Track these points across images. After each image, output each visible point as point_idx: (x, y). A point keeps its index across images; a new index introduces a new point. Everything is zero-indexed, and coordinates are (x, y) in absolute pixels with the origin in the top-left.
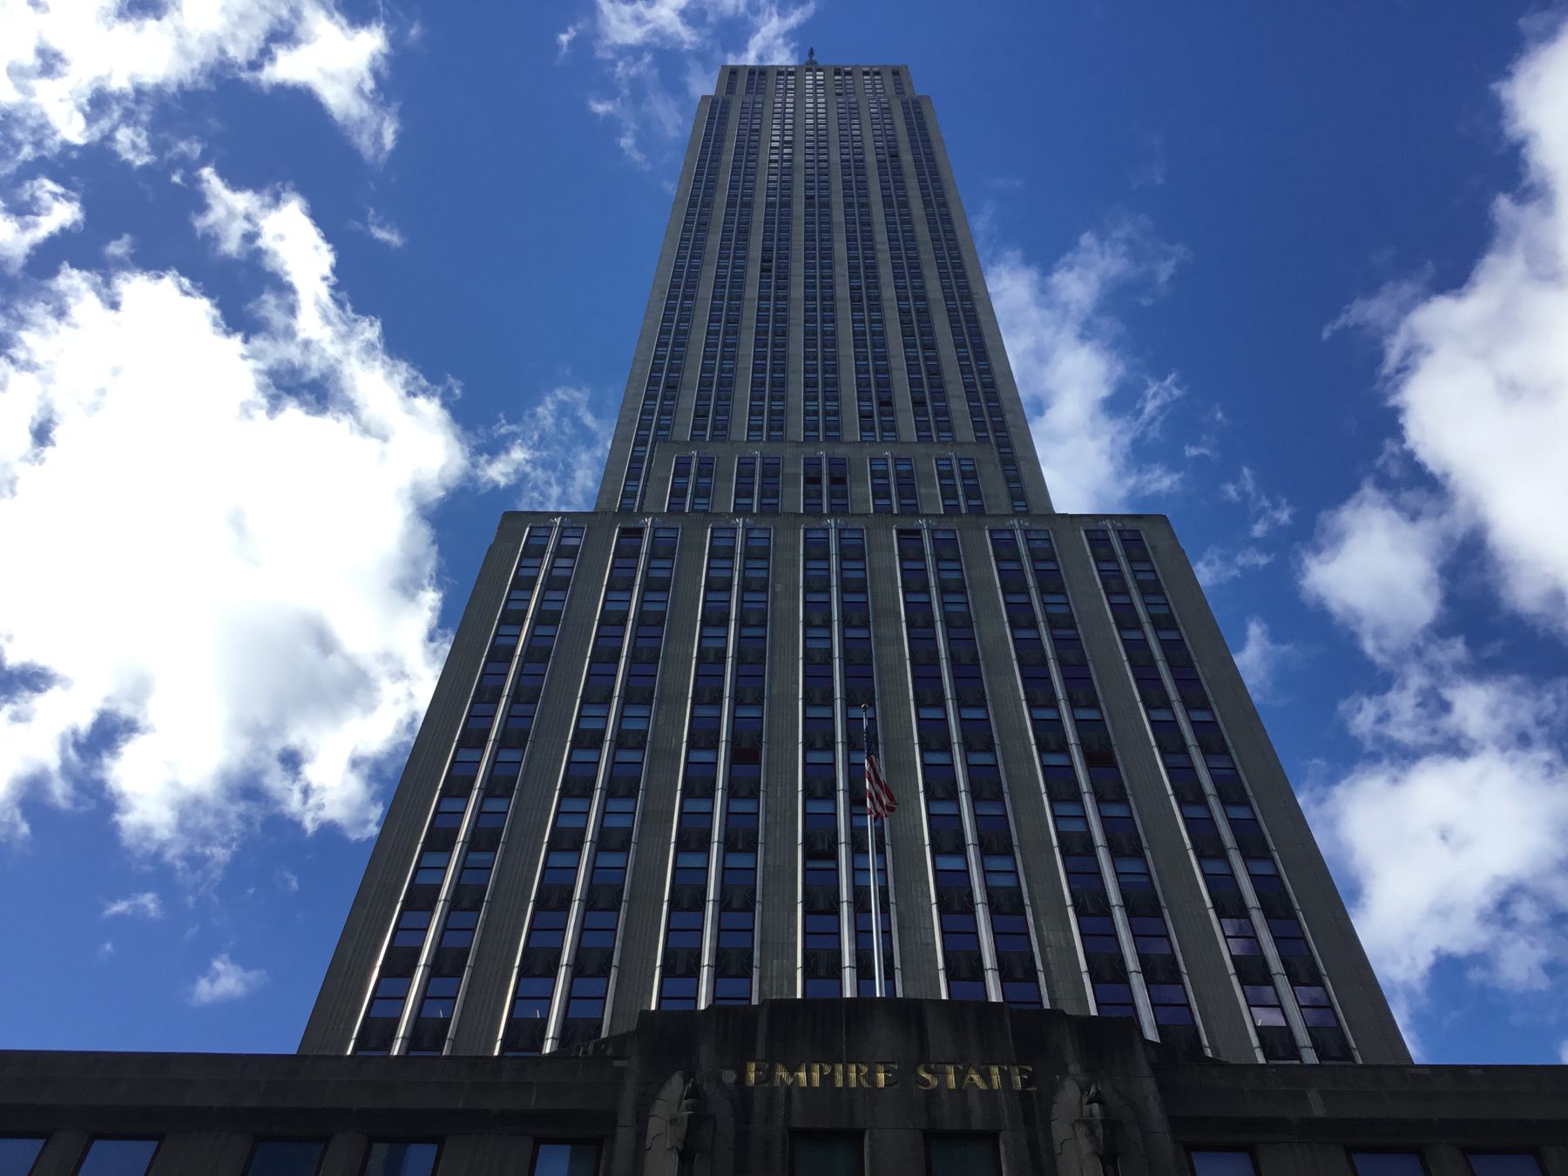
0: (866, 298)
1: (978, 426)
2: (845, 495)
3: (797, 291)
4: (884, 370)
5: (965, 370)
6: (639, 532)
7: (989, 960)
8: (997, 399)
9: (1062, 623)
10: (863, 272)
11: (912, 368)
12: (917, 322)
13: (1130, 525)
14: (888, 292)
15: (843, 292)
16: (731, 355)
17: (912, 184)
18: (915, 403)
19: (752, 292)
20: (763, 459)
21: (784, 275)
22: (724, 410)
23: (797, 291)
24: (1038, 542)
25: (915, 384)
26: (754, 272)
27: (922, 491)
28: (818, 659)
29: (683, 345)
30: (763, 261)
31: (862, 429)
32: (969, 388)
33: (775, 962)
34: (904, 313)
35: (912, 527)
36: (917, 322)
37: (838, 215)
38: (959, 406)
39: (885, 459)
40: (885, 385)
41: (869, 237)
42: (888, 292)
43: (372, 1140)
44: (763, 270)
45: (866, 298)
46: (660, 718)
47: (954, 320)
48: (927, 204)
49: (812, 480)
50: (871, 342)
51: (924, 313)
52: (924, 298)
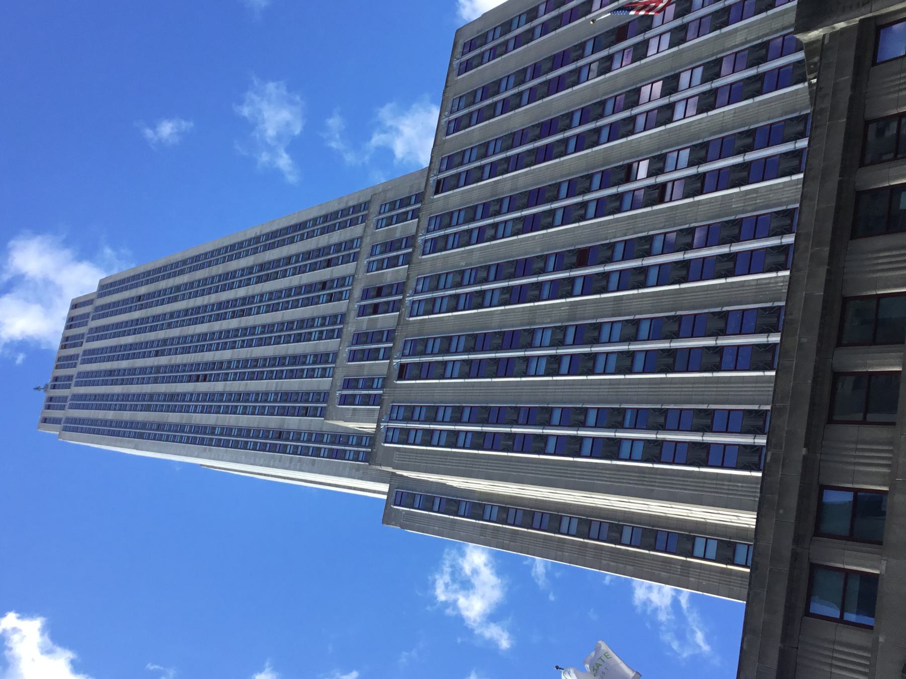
0: (243, 307)
1: (353, 223)
2: (391, 286)
3: (227, 355)
4: (299, 290)
5: (310, 235)
6: (403, 367)
7: (710, 342)
8: (337, 213)
9: (521, 76)
10: (221, 311)
11: (301, 270)
12: (266, 271)
13: (459, 49)
14: (242, 292)
15: (234, 323)
16: (264, 396)
17: (163, 284)
18: (328, 266)
19: (219, 386)
20: (352, 345)
21: (212, 365)
22: (304, 396)
23: (227, 355)
24: (461, 104)
25: (313, 268)
26: (203, 387)
27: (398, 235)
28: (520, 226)
29: (249, 431)
30: (197, 381)
31: (340, 299)
32: (324, 231)
33: (733, 206)
34: (259, 280)
35: (435, 187)
36: (266, 271)
37: (175, 332)
38: (336, 237)
39: (369, 263)
40: (310, 287)
41: (197, 310)
42: (242, 292)
43: (807, 613)
44: (205, 380)
45: (243, 307)
46: (545, 321)
47: (271, 247)
48: (182, 272)
49: (376, 309)
50: (274, 301)
51: (262, 267)
52: (252, 268)
